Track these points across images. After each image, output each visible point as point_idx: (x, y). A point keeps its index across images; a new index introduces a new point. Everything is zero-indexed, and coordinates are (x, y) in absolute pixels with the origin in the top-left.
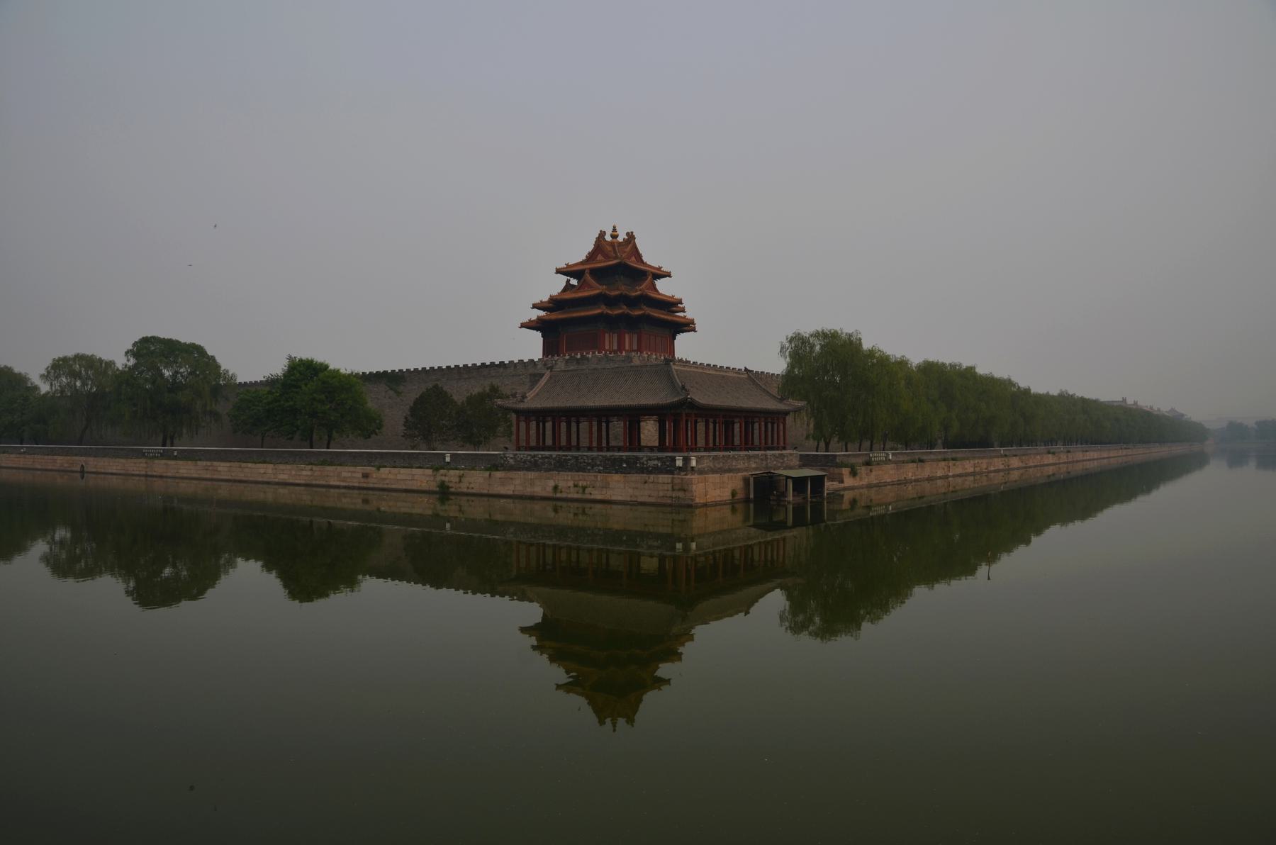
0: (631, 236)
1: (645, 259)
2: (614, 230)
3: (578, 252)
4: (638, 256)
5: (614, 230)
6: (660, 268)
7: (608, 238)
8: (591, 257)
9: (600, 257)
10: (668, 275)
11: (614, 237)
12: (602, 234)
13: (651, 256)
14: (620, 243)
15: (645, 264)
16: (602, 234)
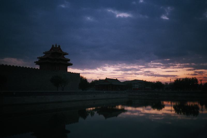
0: (59, 46)
1: (63, 51)
2: (56, 45)
3: (48, 49)
4: (61, 50)
5: (56, 45)
6: (66, 53)
7: (55, 46)
8: (51, 50)
9: (52, 50)
10: (68, 54)
11: (56, 46)
12: (53, 46)
13: (64, 50)
14: (57, 47)
15: (63, 52)
16: (53, 46)
